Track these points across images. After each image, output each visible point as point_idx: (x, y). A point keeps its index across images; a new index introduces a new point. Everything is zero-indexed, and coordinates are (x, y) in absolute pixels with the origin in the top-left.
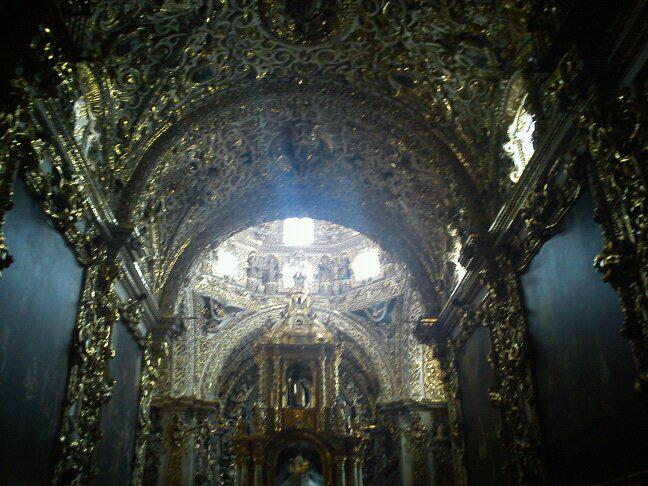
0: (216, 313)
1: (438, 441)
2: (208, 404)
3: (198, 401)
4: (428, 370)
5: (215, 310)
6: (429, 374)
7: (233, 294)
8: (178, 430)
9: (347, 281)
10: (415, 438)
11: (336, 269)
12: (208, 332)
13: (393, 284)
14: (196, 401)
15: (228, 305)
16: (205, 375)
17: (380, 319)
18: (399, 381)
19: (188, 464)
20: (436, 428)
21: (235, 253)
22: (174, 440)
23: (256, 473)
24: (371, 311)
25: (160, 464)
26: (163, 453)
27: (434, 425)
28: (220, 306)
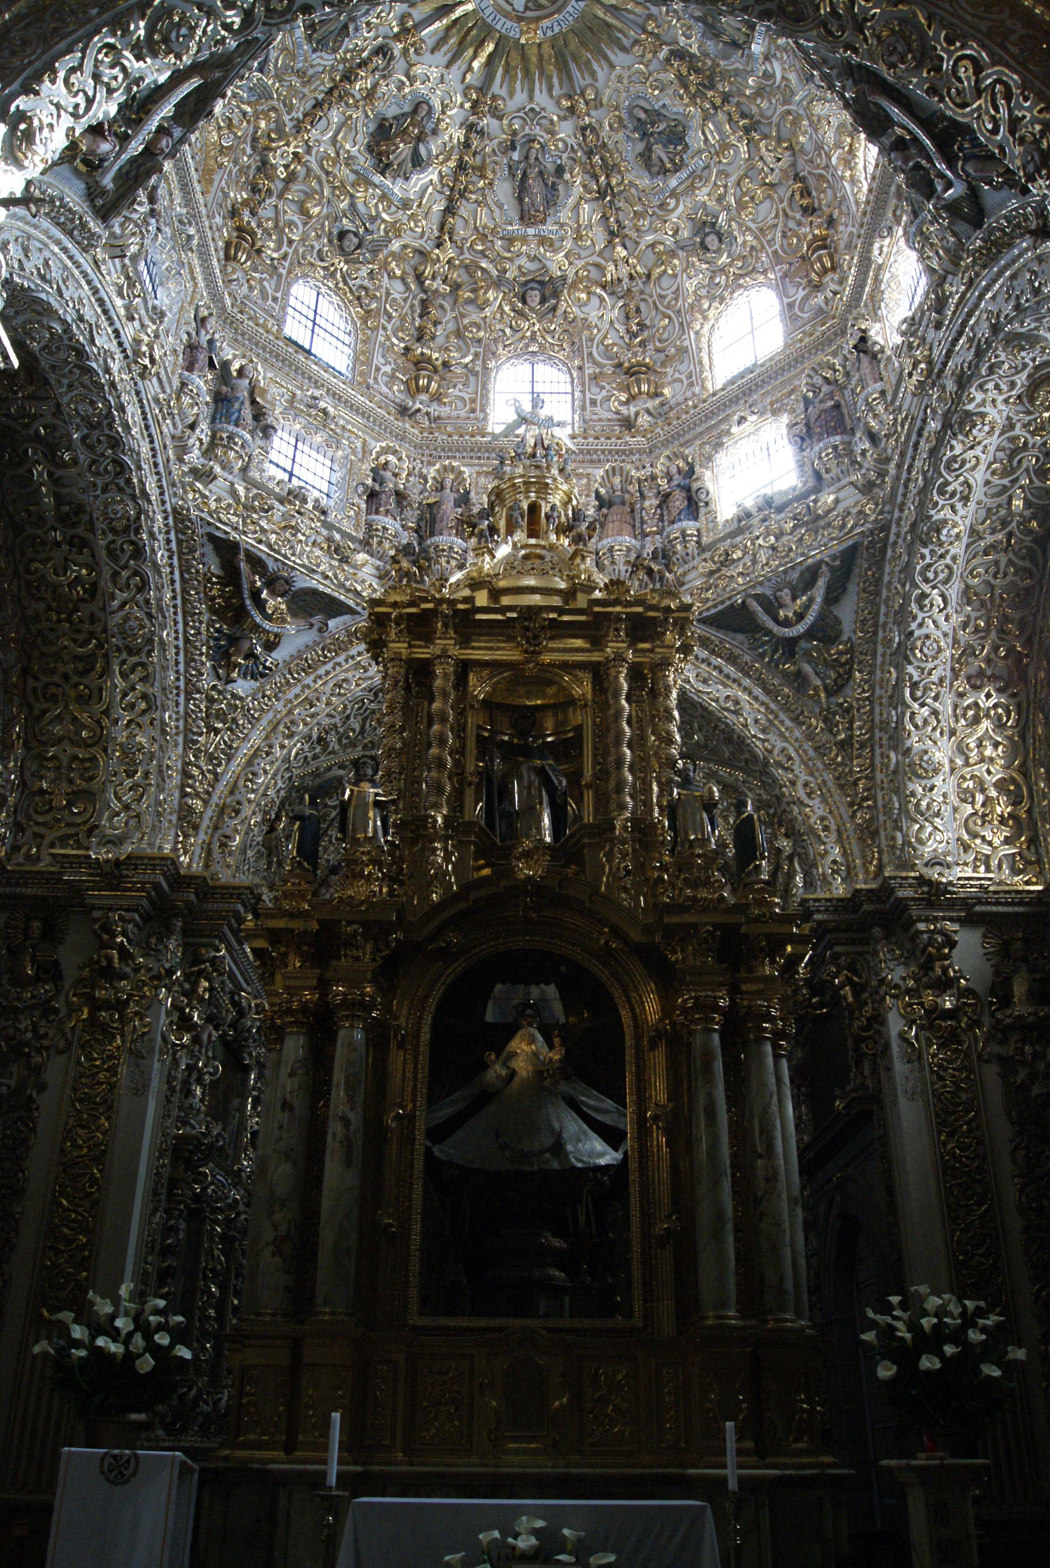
0: (260, 605)
1: (1020, 1025)
2: (233, 892)
3: (188, 881)
4: (967, 797)
5: (256, 595)
6: (969, 809)
7: (318, 552)
8: (110, 974)
9: (690, 526)
10: (935, 1013)
11: (651, 502)
12: (231, 666)
13: (851, 498)
14: (179, 880)
15: (303, 582)
16: (222, 811)
17: (800, 628)
18: (869, 832)
19: (140, 1091)
20: (1008, 980)
21: (334, 442)
22: (96, 1006)
23: (340, 1053)
24: (771, 606)
25: (42, 1088)
26: (60, 1052)
27: (997, 973)
28: (272, 582)
